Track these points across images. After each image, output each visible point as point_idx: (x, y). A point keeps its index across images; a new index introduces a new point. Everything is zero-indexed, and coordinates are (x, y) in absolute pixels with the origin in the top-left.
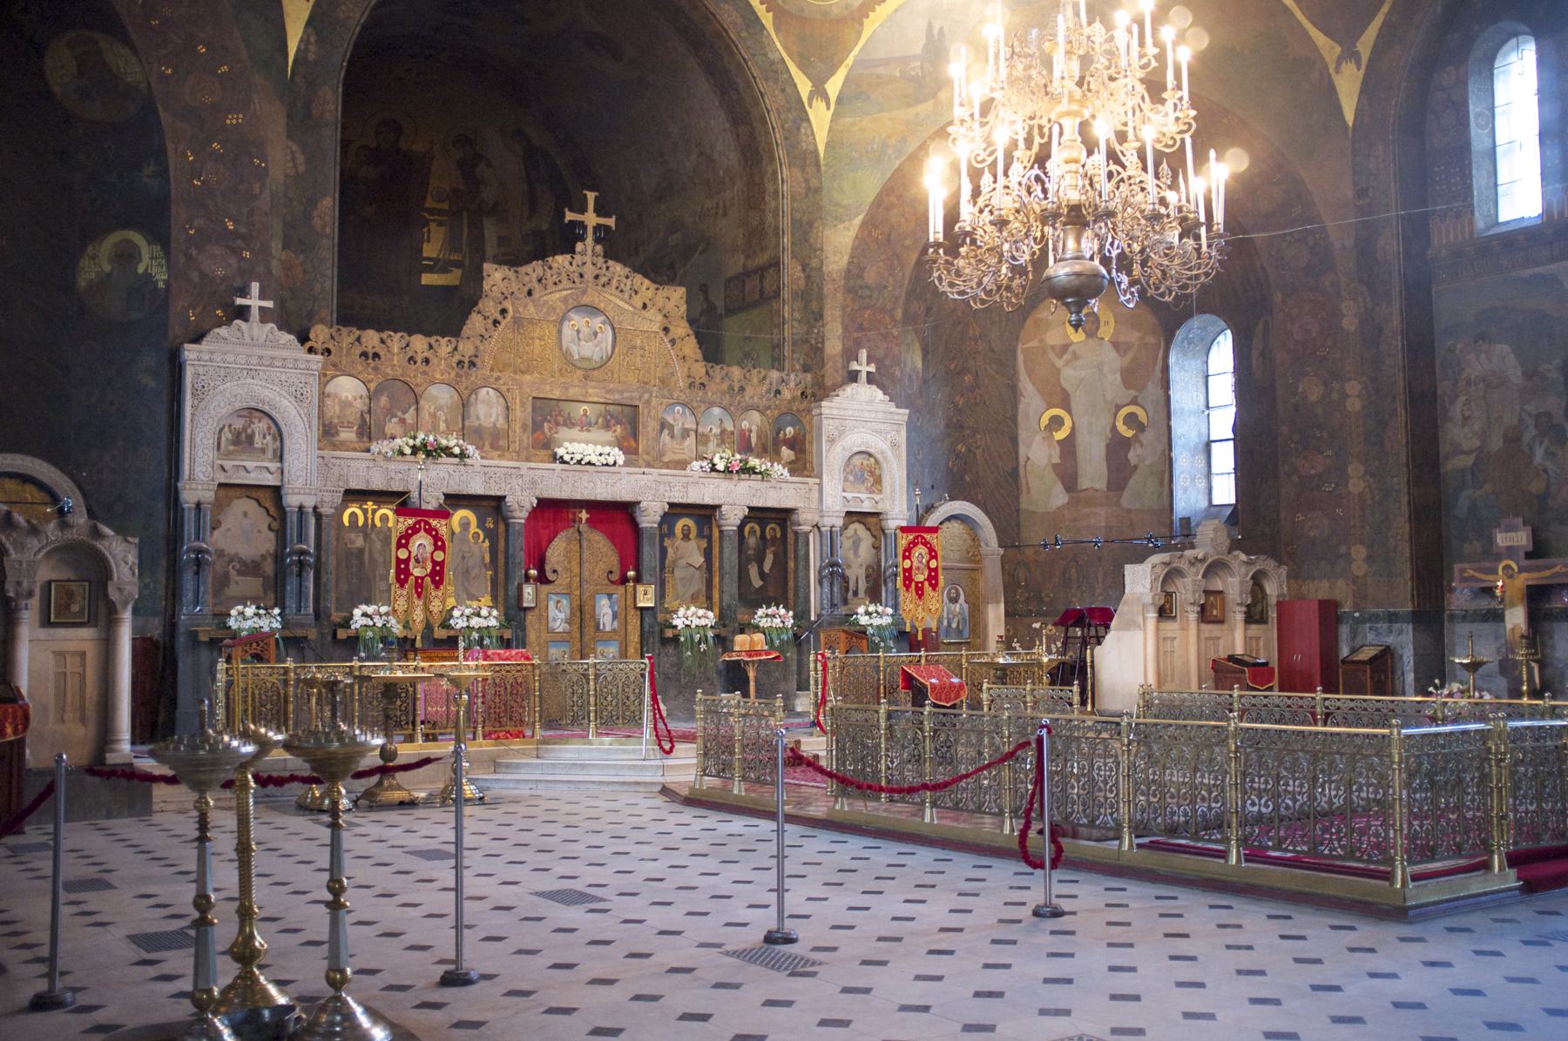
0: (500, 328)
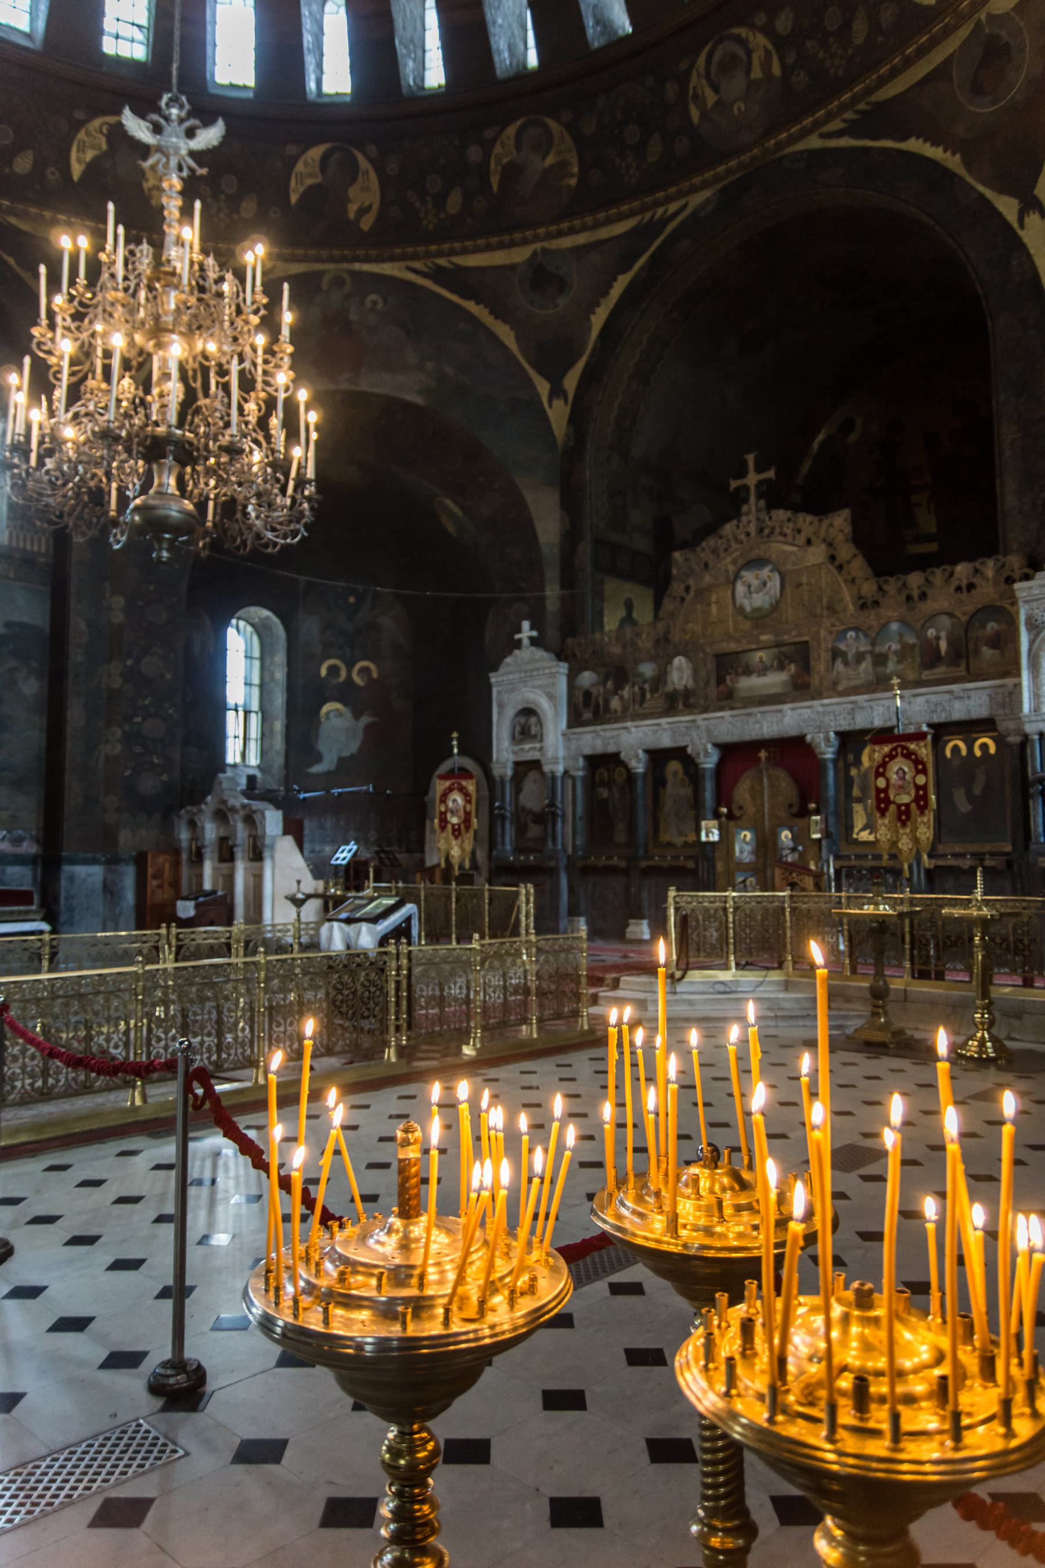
0: (686, 603)
